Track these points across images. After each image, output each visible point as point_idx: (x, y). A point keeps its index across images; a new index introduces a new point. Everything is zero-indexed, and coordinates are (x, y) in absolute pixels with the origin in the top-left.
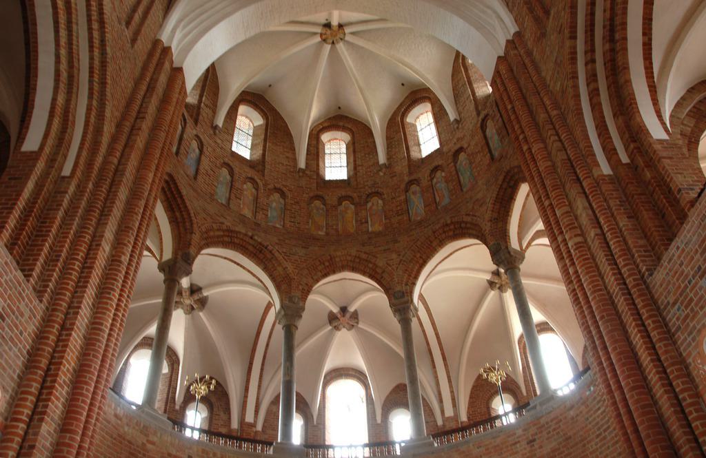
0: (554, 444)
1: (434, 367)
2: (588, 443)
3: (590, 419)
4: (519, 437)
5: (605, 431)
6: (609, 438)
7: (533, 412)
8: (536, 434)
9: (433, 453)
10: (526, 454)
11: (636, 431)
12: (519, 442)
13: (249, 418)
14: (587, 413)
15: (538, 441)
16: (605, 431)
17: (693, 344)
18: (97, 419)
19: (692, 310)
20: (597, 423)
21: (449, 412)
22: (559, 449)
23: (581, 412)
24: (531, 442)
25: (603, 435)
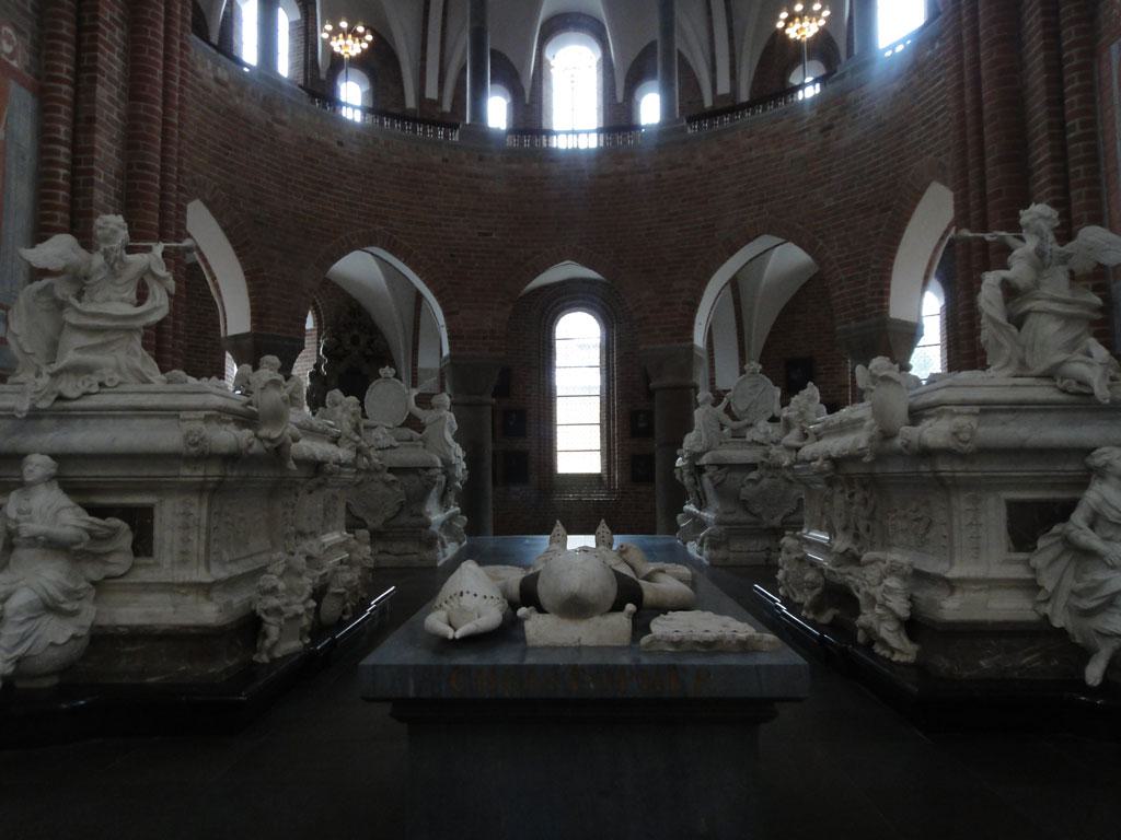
1: (709, 13)
5: (938, 114)
6: (940, 125)
7: (838, 84)
8: (836, 118)
13: (431, 92)
15: (837, 128)
18: (182, 82)
21: (724, 87)
24: (826, 129)
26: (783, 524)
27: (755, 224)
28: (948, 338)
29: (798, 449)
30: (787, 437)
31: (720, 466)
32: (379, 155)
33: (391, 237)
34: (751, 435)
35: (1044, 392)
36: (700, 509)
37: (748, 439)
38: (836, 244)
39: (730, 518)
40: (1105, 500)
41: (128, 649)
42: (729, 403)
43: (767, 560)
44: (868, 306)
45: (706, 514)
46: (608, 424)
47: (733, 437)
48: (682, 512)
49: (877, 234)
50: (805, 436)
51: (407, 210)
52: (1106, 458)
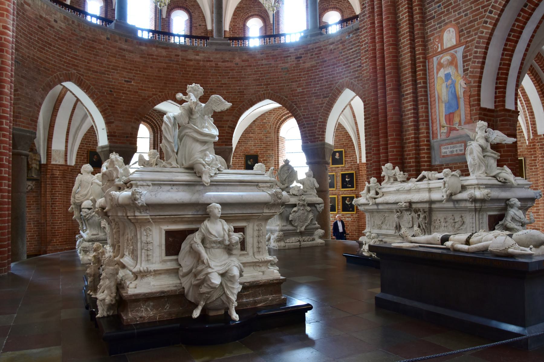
0: (314, 63)
2: (337, 67)
3: (343, 54)
4: (290, 53)
5: (351, 62)
6: (352, 67)
8: (303, 54)
9: (230, 51)
10: (293, 65)
11: (383, 68)
12: (290, 56)
14: (342, 49)
16: (351, 62)
17: (438, 30)
19: (448, 10)
20: (348, 57)
22: (316, 66)
23: (338, 48)
24: (298, 58)
25: (349, 65)
26: (305, 229)
27: (264, 94)
29: (375, 198)
32: (74, 30)
35: (495, 182)
39: (285, 228)
40: (515, 214)
43: (300, 245)
44: (317, 136)
49: (322, 107)
50: (377, 193)
51: (88, 63)
52: (514, 201)
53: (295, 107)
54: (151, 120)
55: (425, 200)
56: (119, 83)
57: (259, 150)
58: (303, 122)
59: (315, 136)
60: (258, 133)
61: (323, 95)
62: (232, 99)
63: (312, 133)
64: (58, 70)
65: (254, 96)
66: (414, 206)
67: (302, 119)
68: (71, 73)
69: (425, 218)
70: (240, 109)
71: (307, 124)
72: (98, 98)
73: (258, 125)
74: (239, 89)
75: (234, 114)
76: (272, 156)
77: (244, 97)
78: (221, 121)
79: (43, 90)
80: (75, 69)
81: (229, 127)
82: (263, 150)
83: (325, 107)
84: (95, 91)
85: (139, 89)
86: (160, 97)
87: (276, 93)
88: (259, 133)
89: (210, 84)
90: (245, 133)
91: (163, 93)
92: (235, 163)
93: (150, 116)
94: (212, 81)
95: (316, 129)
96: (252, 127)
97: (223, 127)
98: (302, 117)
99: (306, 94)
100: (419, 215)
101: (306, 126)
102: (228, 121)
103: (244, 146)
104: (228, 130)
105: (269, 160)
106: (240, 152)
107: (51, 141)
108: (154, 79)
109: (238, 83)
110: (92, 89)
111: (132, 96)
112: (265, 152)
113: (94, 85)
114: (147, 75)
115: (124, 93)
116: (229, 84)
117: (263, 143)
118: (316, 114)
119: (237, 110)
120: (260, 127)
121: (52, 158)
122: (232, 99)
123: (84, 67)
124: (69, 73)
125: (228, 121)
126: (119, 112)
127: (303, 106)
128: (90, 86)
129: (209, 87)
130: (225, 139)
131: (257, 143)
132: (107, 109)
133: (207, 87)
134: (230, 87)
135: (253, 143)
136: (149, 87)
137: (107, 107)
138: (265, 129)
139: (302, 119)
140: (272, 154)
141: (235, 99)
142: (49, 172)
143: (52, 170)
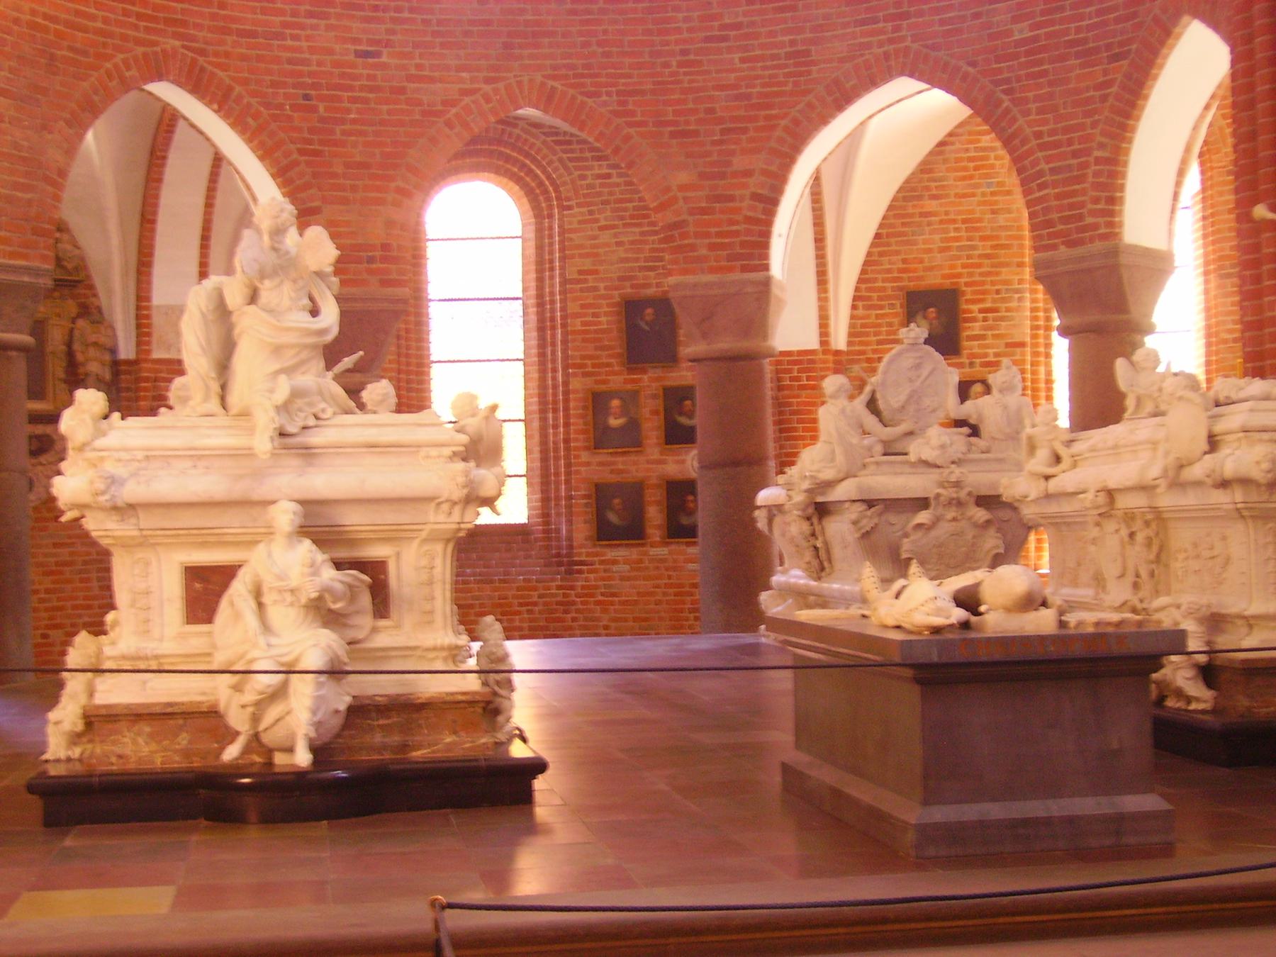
27: (887, 56)
28: (1206, 255)
29: (1047, 478)
30: (1033, 461)
31: (870, 503)
33: (194, 61)
34: (918, 449)
36: (819, 579)
37: (912, 457)
38: (1033, 106)
41: (381, 722)
42: (873, 393)
44: (1089, 220)
45: (836, 586)
46: (543, 420)
47: (885, 454)
48: (768, 587)
49: (1104, 98)
53: (1006, 104)
54: (523, 166)
55: (1129, 483)
56: (337, 64)
57: (964, 266)
58: (1035, 163)
59: (1080, 217)
60: (957, 195)
61: (1109, 47)
62: (764, 85)
63: (1071, 207)
64: (118, 49)
65: (848, 66)
66: (1124, 502)
67: (1030, 153)
68: (164, 51)
69: (1149, 543)
70: (796, 122)
71: (1053, 171)
72: (261, 128)
73: (958, 160)
74: (792, 43)
75: (773, 144)
76: (1017, 291)
77: (809, 73)
78: (722, 176)
79: (69, 123)
80: (176, 36)
81: (756, 197)
82: (979, 265)
83: (1118, 97)
84: (249, 105)
85: (410, 78)
86: (488, 100)
87: (934, 48)
88: (964, 196)
89: (679, 31)
90: (905, 199)
91: (501, 85)
92: (863, 326)
93: (520, 151)
94: (686, 19)
95: (1084, 192)
96: (930, 171)
97: (731, 198)
98: (1034, 143)
99: (1044, 49)
100: (1132, 535)
101: (1048, 178)
102: (748, 173)
103: (897, 253)
104: (752, 208)
105: (1008, 310)
106: (884, 280)
107: (149, 274)
108: (467, 34)
109: (785, 21)
110: (239, 99)
111: (385, 108)
112: (989, 274)
113: (245, 82)
114: (440, 23)
115: (353, 100)
116: (753, 24)
117: (983, 238)
118: (1081, 127)
119: (786, 129)
120: (965, 169)
121: (155, 339)
122: (764, 85)
123: (207, 22)
124: (156, 53)
125: (748, 173)
126: (339, 169)
127: (1037, 99)
128: (230, 89)
129: (677, 42)
130: (743, 244)
131: (957, 239)
132: (295, 164)
133: (667, 43)
134: (756, 36)
135: (937, 237)
136: (448, 68)
137: (295, 156)
138: (987, 176)
139: (1030, 153)
140: (1021, 282)
141: (779, 84)
142: (146, 389)
143: (156, 380)
